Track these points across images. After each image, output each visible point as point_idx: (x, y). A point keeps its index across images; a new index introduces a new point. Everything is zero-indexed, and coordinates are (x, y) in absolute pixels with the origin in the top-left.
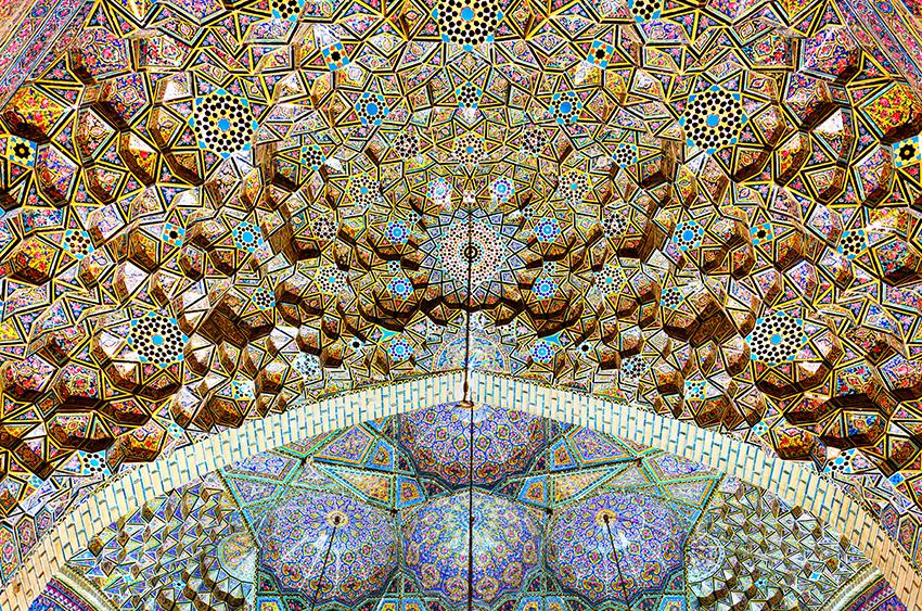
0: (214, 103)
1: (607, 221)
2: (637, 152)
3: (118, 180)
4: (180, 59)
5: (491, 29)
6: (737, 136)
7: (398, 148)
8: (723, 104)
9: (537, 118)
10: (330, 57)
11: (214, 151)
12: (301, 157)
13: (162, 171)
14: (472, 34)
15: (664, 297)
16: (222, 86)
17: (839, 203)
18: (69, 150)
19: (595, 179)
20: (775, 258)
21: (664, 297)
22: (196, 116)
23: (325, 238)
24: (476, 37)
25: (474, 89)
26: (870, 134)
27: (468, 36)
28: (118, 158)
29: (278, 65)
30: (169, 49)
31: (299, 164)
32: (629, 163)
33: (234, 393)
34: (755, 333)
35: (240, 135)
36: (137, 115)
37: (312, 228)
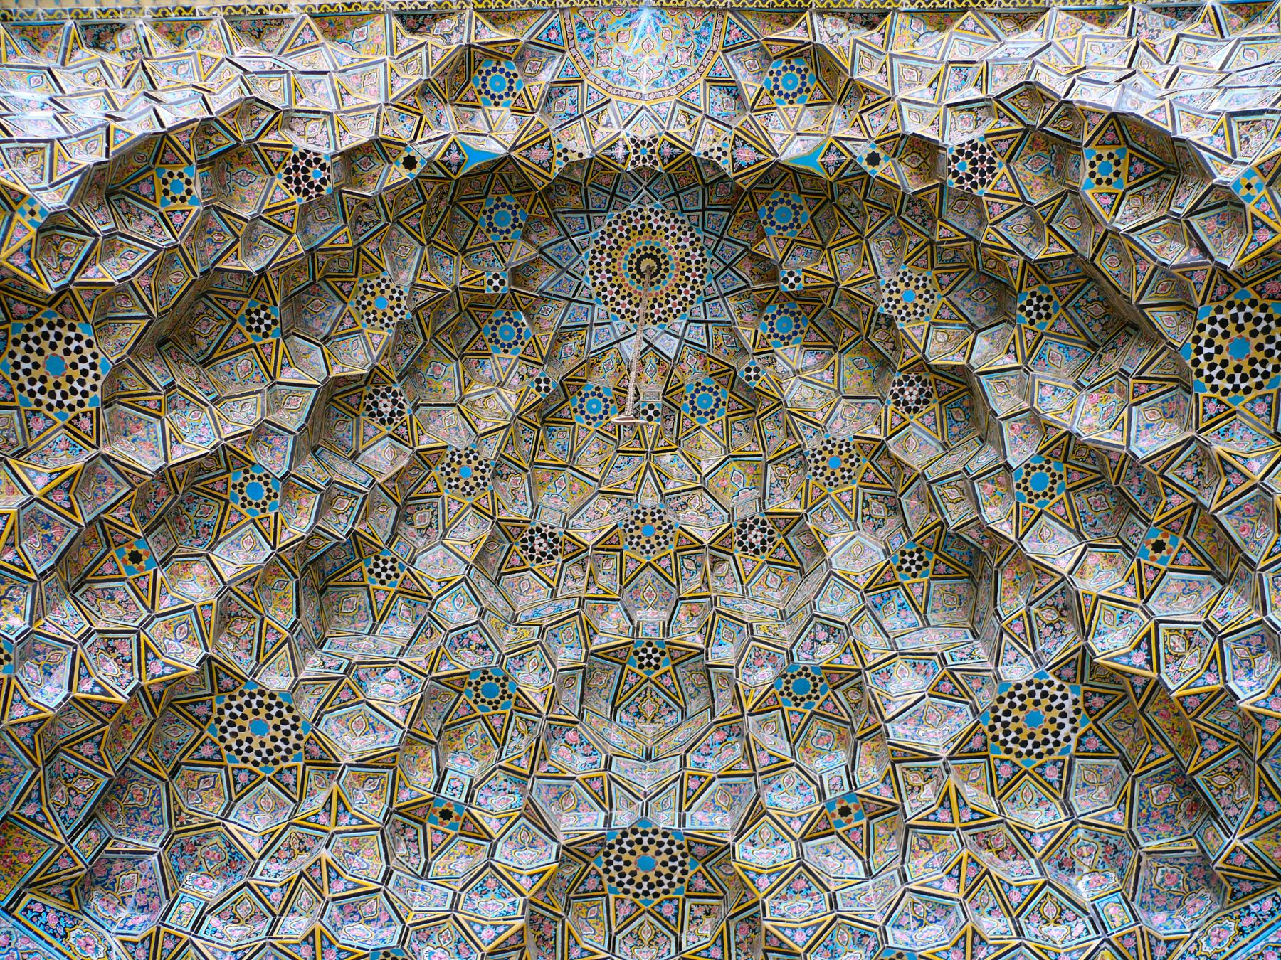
0: (1042, 749)
1: (400, 413)
2: (366, 575)
3: (1212, 711)
4: (1073, 840)
5: (611, 846)
6: (216, 706)
7: (771, 532)
8: (249, 750)
9: (536, 653)
10: (853, 811)
11: (1057, 683)
12: (932, 563)
13: (1144, 690)
14: (639, 841)
15: (275, 322)
16: (1026, 772)
17: (38, 721)
18: (1267, 788)
19: (429, 487)
20: (102, 527)
21: (275, 322)
22: (1075, 730)
23: (913, 376)
24: (632, 837)
25: (641, 667)
26: (29, 818)
27: (645, 839)
28: (1201, 740)
29: (929, 837)
30: (1086, 854)
31: (936, 551)
32: (377, 558)
33: (1125, 162)
34: (97, 377)
35: (1012, 705)
36: (1160, 769)
37: (935, 396)
